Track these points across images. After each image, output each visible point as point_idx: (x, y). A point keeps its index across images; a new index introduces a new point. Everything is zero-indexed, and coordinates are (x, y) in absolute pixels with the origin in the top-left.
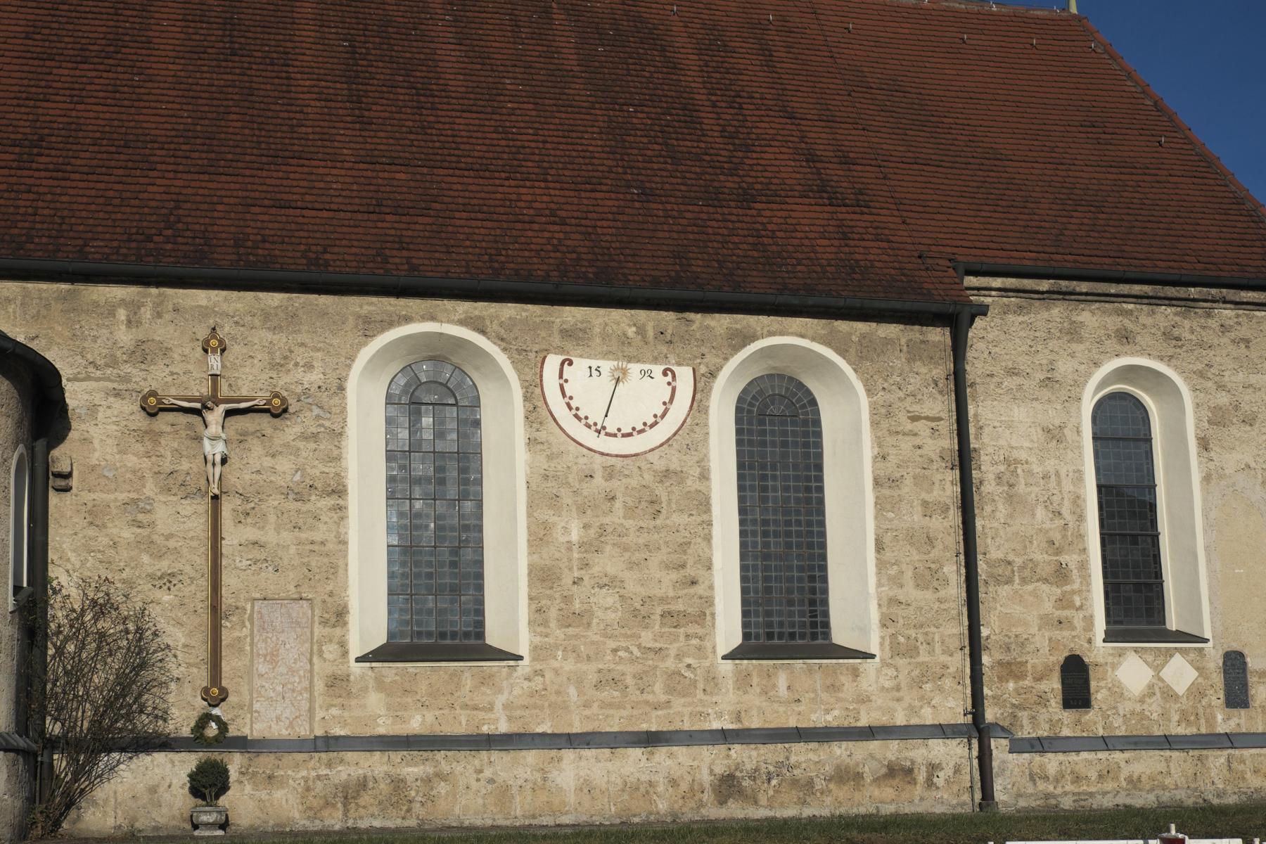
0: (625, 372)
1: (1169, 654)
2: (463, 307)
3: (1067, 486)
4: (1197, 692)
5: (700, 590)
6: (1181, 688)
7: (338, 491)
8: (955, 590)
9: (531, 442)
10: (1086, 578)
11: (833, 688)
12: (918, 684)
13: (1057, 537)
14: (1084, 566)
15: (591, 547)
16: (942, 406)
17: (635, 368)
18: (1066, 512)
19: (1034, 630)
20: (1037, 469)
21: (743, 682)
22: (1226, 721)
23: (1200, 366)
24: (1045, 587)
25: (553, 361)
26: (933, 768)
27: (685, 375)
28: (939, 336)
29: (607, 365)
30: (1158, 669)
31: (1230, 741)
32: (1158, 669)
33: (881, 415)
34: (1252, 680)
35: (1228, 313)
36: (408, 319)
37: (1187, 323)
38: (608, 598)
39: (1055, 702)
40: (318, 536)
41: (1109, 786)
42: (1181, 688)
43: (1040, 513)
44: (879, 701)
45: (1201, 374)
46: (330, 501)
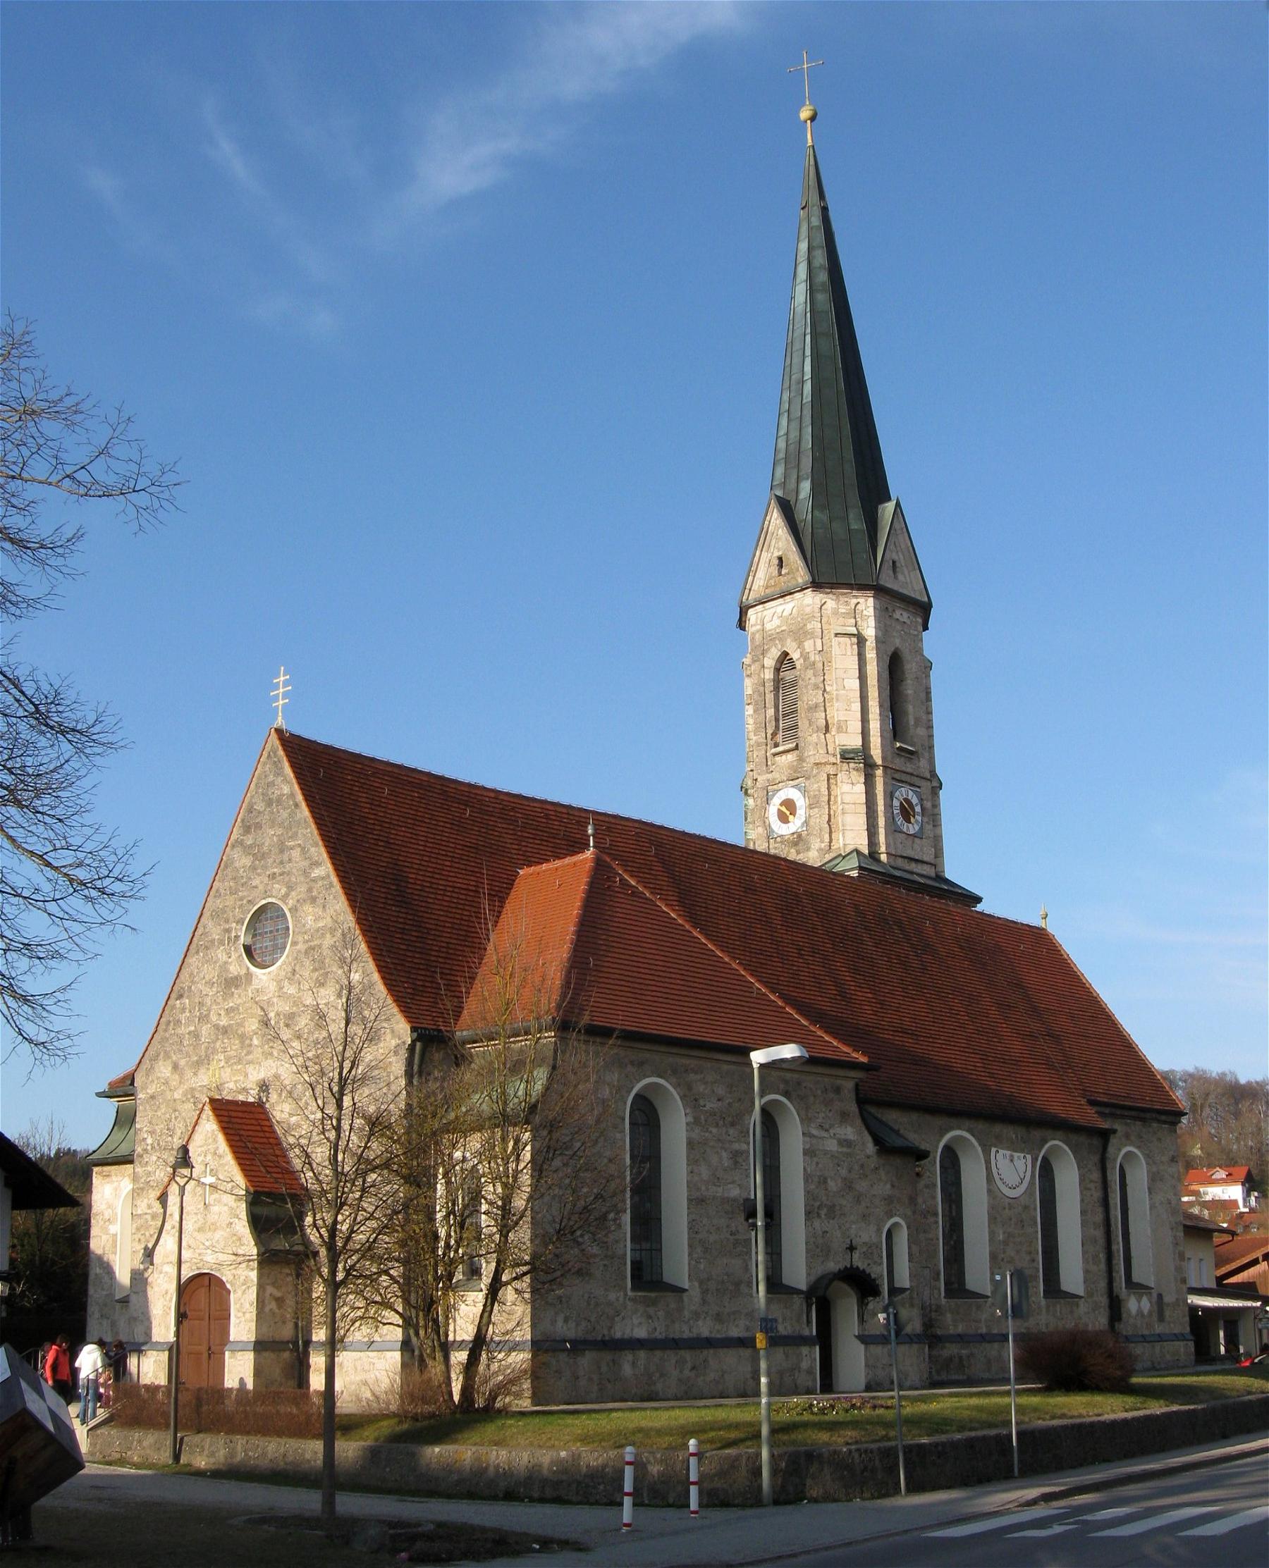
0: (1012, 1156)
1: (1141, 1296)
2: (967, 1123)
4: (1150, 1313)
6: (1146, 1312)
7: (936, 1214)
8: (1103, 1266)
9: (989, 1191)
11: (1072, 1312)
12: (1094, 1310)
15: (1005, 1243)
16: (1096, 1175)
17: (1016, 1155)
21: (1048, 1307)
22: (1159, 1329)
25: (993, 1150)
27: (1029, 1157)
28: (1096, 1142)
29: (1008, 1153)
30: (1139, 1302)
31: (1160, 1338)
32: (1139, 1302)
33: (1082, 1180)
35: (1155, 1125)
36: (952, 1129)
40: (931, 1236)
42: (1146, 1312)
46: (932, 1219)
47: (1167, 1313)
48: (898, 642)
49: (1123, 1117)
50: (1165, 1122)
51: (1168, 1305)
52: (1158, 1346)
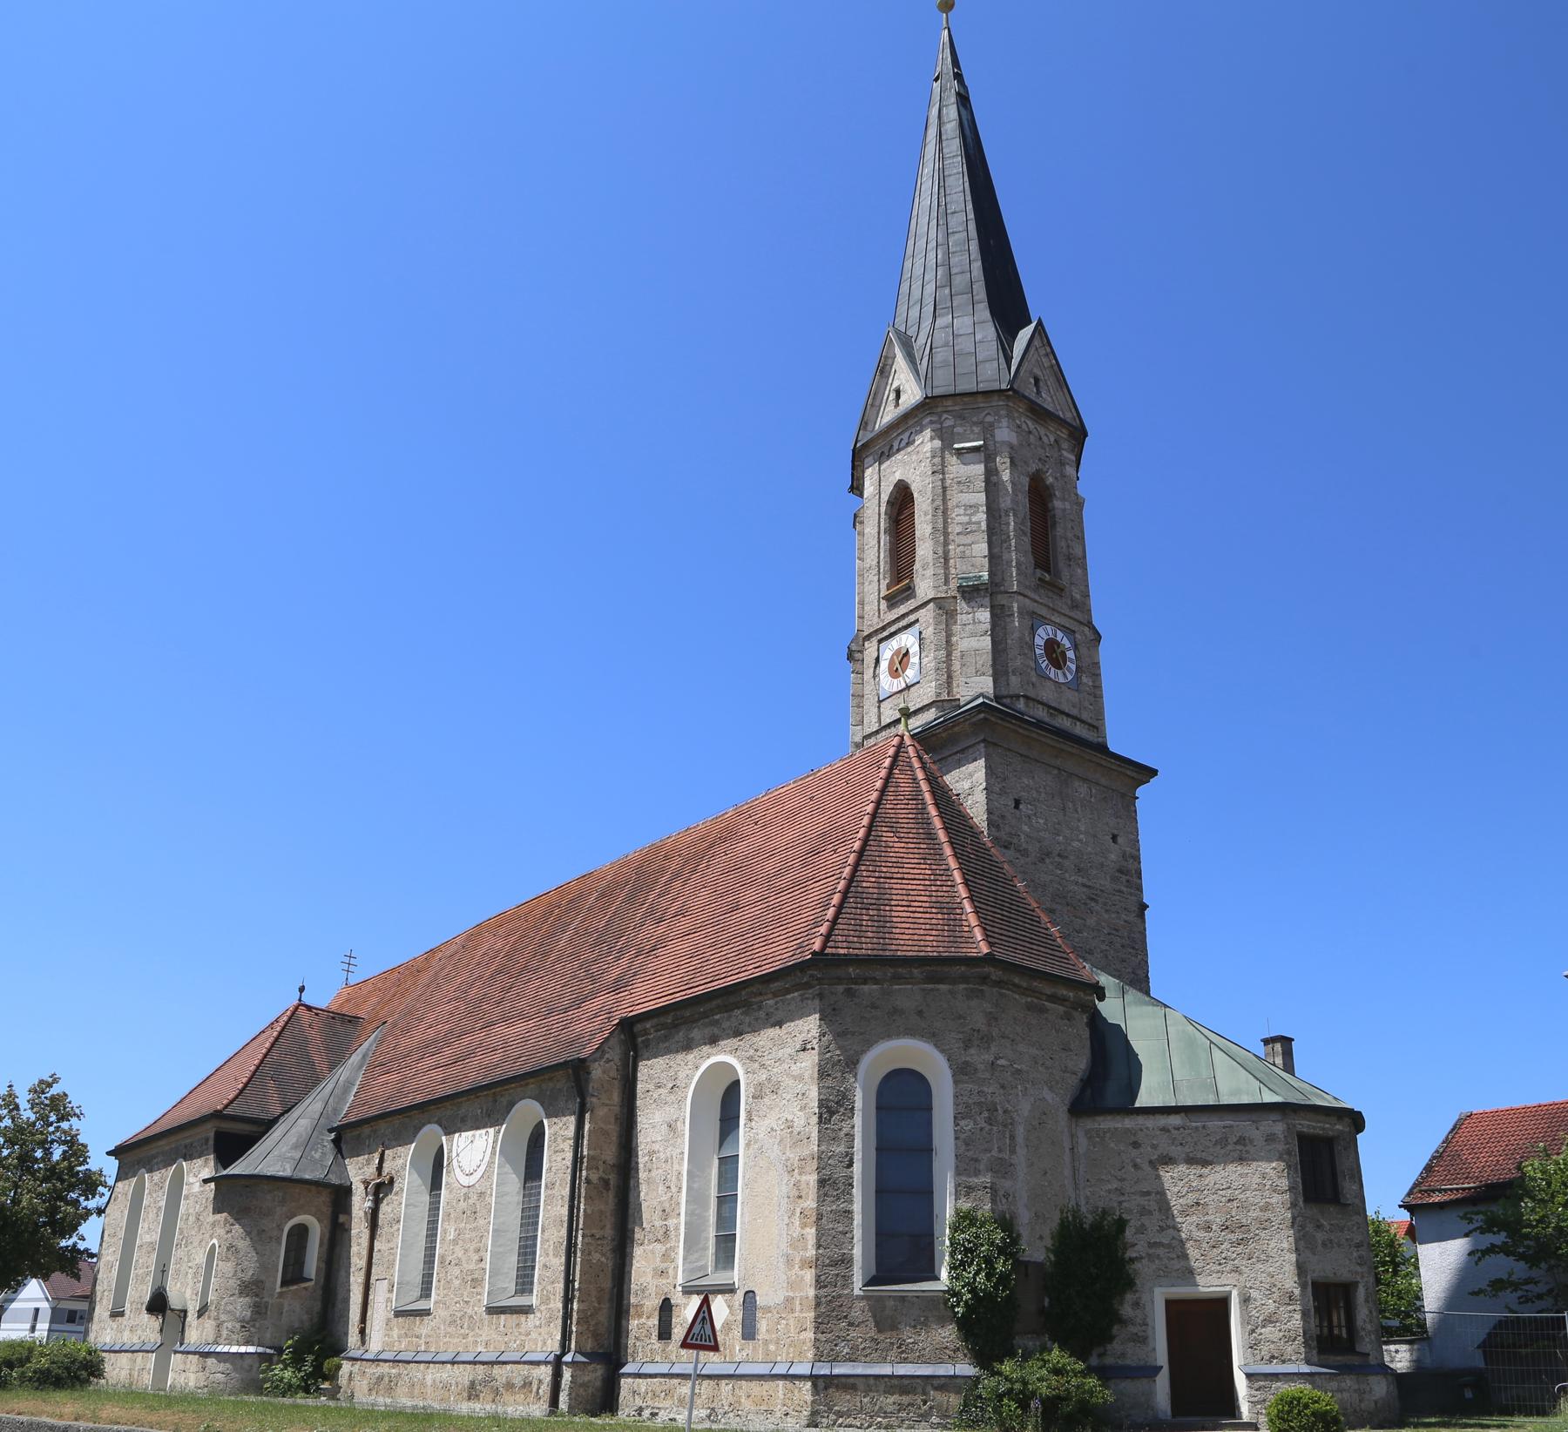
3: (676, 1167)
5: (482, 1265)
10: (678, 1236)
13: (667, 1205)
14: (677, 1229)
18: (674, 1189)
19: (649, 1279)
20: (662, 1156)
23: (752, 1052)
24: (658, 1246)
26: (540, 1381)
34: (759, 1315)
37: (747, 1020)
38: (456, 1271)
39: (655, 1333)
41: (667, 1403)
43: (661, 1188)
44: (534, 1335)
45: (751, 1058)
47: (763, 1326)
48: (898, 476)
49: (705, 1015)
50: (788, 991)
51: (768, 1309)
52: (726, 1387)
